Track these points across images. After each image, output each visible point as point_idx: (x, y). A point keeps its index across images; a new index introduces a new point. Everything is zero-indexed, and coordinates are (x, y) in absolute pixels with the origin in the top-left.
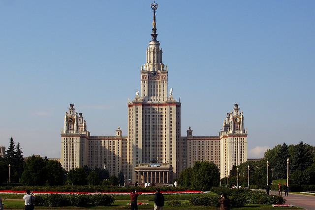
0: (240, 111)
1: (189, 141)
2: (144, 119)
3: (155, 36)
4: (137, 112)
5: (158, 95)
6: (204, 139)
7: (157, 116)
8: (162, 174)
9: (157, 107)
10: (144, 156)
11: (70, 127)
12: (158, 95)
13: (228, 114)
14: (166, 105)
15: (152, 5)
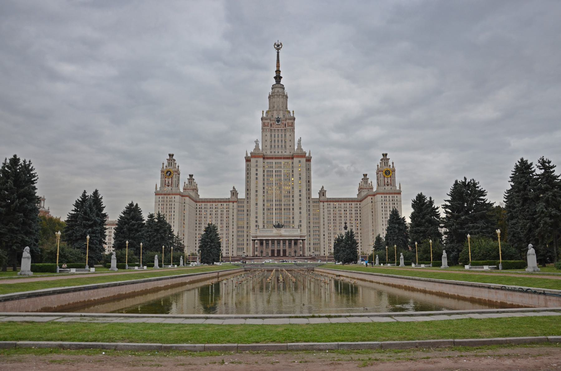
0: (390, 163)
1: (321, 204)
2: (266, 176)
3: (278, 78)
4: (257, 165)
5: (283, 146)
6: (341, 201)
8: (290, 244)
9: (283, 161)
10: (266, 222)
13: (364, 175)
14: (292, 158)
15: (275, 44)
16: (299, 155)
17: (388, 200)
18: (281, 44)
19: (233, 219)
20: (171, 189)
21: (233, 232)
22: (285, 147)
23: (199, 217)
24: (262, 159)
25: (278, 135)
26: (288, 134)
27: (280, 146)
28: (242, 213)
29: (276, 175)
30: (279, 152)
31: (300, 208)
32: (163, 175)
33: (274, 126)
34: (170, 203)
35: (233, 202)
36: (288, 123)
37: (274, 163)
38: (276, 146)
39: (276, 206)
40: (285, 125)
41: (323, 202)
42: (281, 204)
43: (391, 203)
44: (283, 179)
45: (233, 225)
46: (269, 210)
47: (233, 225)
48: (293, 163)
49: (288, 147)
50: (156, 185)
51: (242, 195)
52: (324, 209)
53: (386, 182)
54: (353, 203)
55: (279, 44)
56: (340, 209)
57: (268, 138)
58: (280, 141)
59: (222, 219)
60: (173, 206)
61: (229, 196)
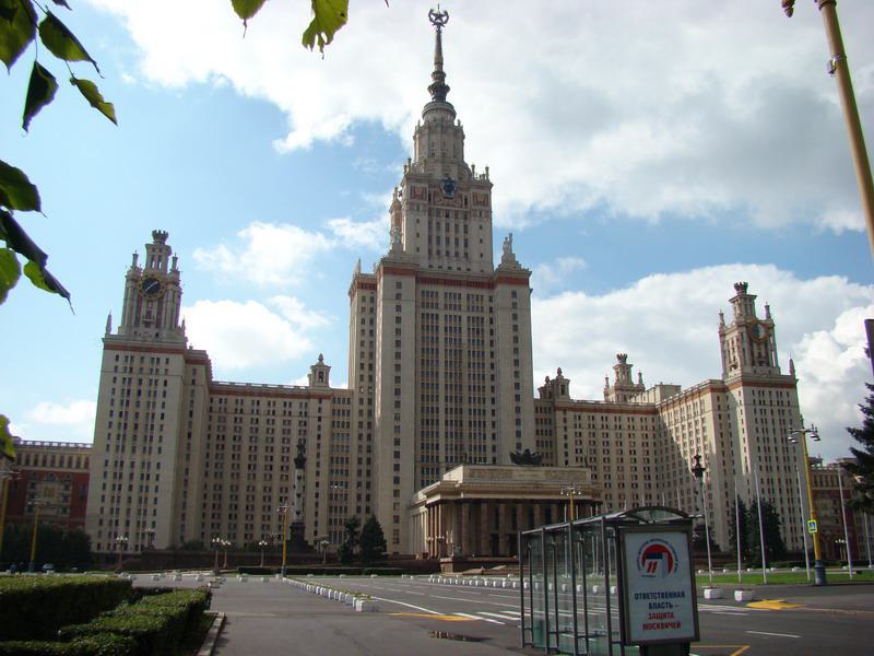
3: (439, 89)
4: (398, 296)
5: (462, 254)
7: (464, 319)
9: (464, 291)
11: (144, 311)
12: (462, 254)
14: (491, 285)
15: (431, 11)
16: (513, 276)
17: (768, 403)
18: (446, 13)
19: (319, 445)
20: (157, 335)
21: (317, 484)
22: (466, 255)
23: (218, 437)
24: (412, 280)
25: (447, 225)
26: (474, 224)
27: (452, 253)
28: (345, 431)
29: (446, 328)
30: (456, 266)
31: (518, 422)
32: (135, 289)
33: (437, 199)
34: (151, 377)
35: (320, 399)
36: (475, 196)
37: (441, 296)
38: (443, 253)
39: (446, 412)
40: (466, 200)
41: (565, 413)
42: (461, 410)
43: (776, 409)
44: (465, 338)
45: (318, 464)
46: (428, 423)
47: (318, 464)
48: (491, 300)
49: (475, 256)
50: (110, 316)
51: (340, 380)
52: (565, 428)
53: (756, 355)
54: (637, 417)
55: (442, 13)
56: (605, 431)
57: (423, 229)
58: (452, 241)
59: (285, 445)
60: (160, 388)
61: (303, 382)
